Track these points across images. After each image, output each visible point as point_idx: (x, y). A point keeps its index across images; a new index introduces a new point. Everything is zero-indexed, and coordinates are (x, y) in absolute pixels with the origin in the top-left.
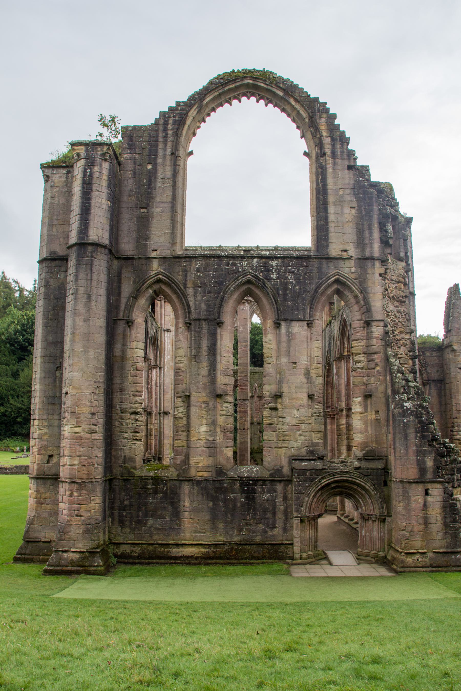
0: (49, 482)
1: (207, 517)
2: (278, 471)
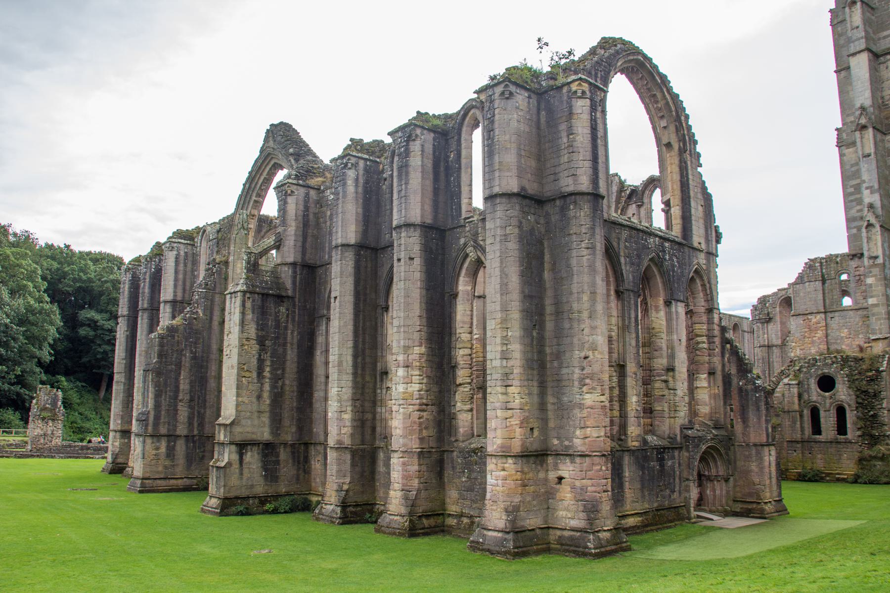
0: (532, 459)
1: (639, 486)
2: (672, 438)
